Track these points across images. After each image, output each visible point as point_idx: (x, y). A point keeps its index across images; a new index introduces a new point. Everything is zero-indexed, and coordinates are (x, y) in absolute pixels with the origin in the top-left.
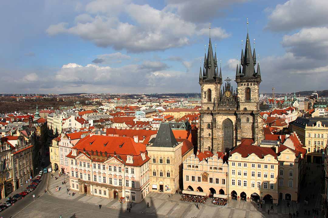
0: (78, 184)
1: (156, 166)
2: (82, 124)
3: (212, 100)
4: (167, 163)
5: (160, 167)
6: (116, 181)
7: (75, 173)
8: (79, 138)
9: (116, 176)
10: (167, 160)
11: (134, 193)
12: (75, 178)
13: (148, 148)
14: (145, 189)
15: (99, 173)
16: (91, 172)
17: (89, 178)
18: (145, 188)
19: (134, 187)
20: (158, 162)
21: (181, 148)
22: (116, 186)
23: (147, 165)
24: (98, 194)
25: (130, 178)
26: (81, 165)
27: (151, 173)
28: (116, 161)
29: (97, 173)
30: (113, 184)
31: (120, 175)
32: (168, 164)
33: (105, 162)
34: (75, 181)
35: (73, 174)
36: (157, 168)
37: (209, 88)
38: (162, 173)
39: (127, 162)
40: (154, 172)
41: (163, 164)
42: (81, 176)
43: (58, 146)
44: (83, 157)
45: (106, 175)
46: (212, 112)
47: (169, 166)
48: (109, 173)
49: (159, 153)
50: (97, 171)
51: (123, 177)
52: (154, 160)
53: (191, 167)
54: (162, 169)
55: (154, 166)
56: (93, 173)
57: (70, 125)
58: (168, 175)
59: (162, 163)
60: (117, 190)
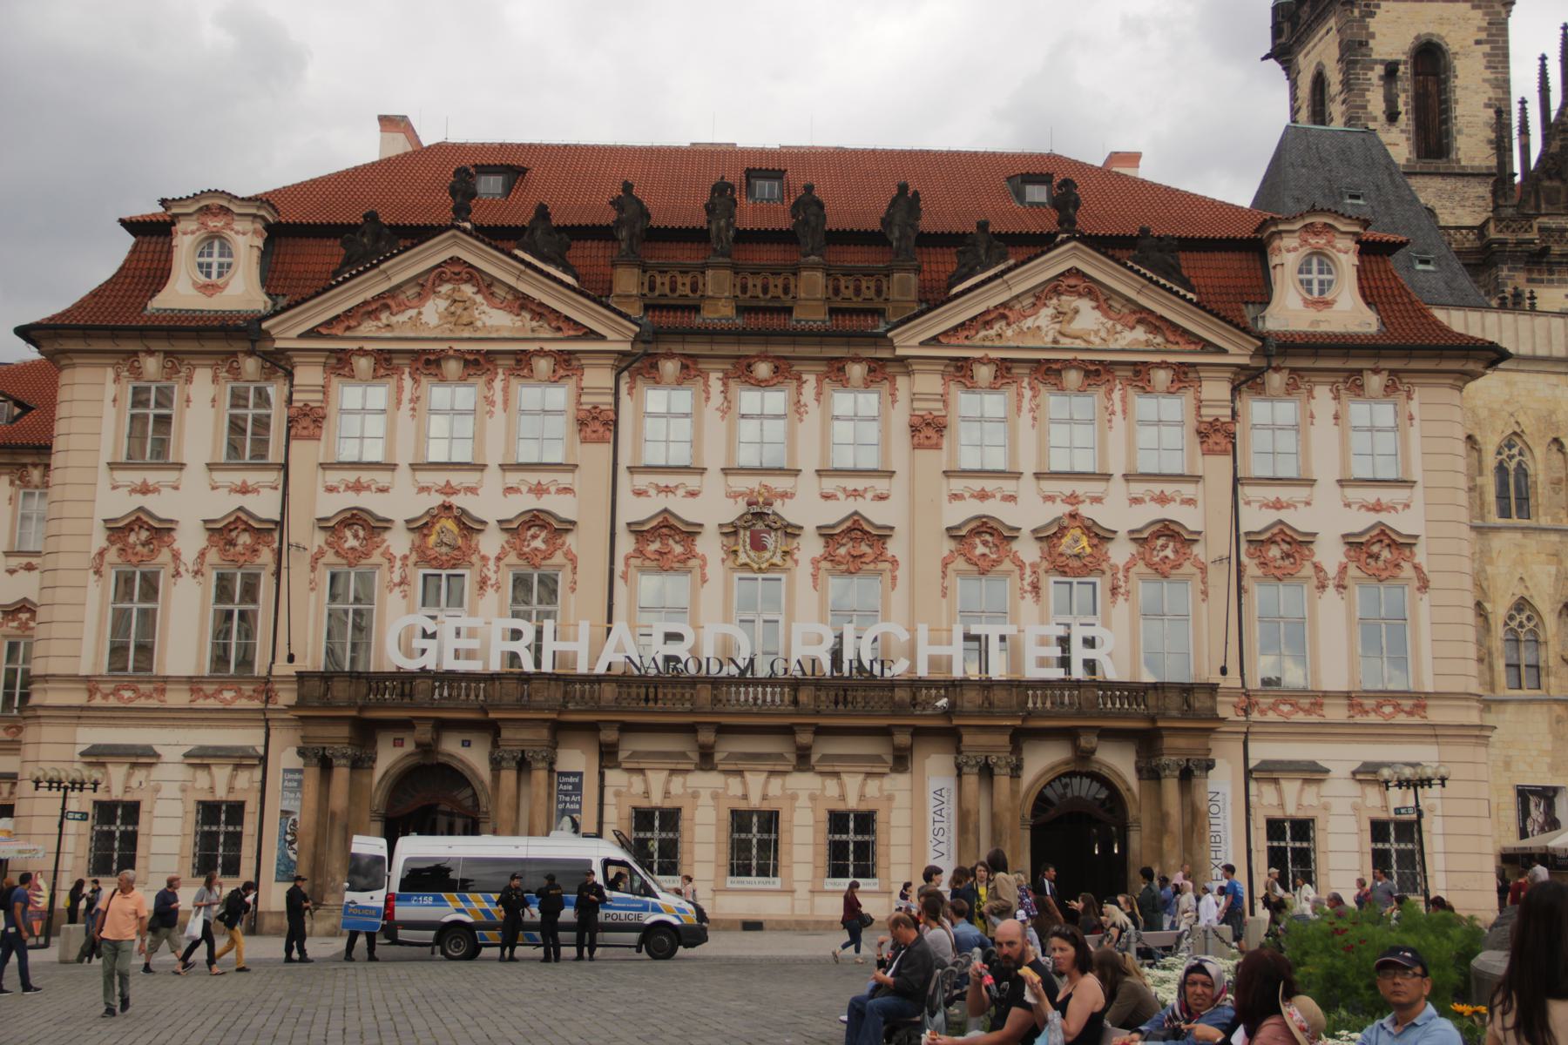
3: (1472, 147)
4: (1504, 512)
10: (1501, 469)
12: (177, 698)
15: (758, 527)
25: (1329, 554)
28: (1088, 318)
29: (710, 546)
31: (1172, 512)
32: (1515, 521)
33: (908, 342)
37: (1424, 30)
39: (1288, 311)
45: (894, 548)
46: (1493, 233)
47: (1532, 543)
48: (969, 509)
50: (712, 507)
51: (1217, 543)
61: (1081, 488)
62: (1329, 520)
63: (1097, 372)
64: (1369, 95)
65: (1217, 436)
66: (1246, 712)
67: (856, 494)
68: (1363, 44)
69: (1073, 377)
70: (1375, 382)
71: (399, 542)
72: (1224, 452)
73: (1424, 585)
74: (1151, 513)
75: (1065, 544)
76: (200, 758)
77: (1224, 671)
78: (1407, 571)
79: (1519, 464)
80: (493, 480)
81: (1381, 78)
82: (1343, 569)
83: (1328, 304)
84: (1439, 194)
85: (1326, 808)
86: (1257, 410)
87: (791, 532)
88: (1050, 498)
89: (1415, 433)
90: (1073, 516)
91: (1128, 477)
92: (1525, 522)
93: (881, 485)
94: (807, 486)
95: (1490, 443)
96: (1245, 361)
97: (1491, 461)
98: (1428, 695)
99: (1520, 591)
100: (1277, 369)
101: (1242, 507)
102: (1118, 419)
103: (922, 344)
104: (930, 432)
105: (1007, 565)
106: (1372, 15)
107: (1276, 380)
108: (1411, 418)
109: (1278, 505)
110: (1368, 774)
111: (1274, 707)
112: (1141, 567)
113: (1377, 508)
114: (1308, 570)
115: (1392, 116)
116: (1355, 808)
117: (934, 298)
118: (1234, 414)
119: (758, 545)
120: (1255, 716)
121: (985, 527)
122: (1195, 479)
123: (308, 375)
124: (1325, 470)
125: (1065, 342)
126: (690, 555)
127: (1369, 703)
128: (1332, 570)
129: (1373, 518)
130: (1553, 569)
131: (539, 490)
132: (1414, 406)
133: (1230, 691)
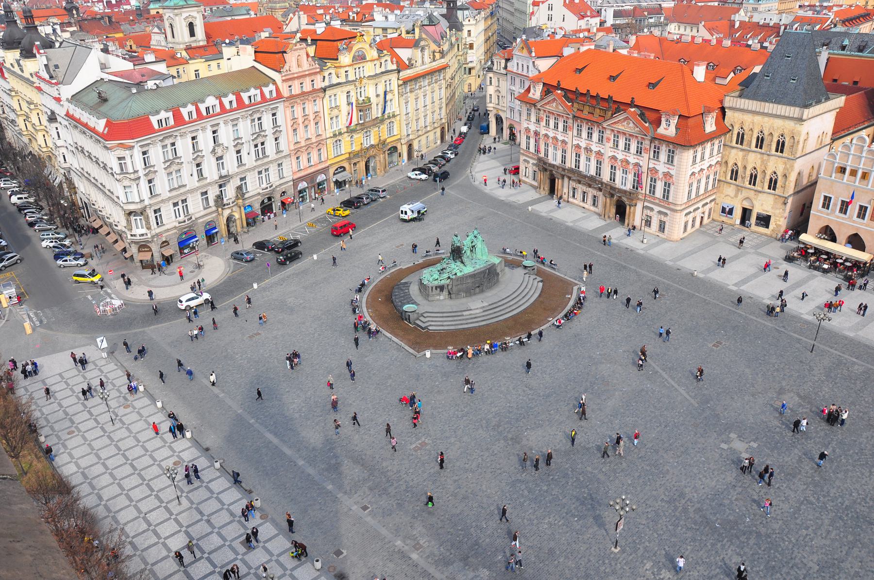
0: (537, 169)
1: (741, 154)
2: (583, 17)
4: (777, 151)
5: (754, 160)
7: (532, 141)
8: (560, 56)
10: (778, 142)
11: (666, 214)
13: (728, 102)
14: (700, 210)
15: (588, 150)
16: (569, 145)
17: (564, 158)
18: (698, 208)
19: (667, 198)
21: (834, 113)
22: (624, 188)
23: (716, 147)
24: (578, 201)
26: (548, 124)
27: (725, 172)
28: (631, 125)
29: (582, 150)
30: (618, 184)
32: (779, 154)
33: (605, 125)
34: (532, 161)
35: (528, 144)
38: (756, 176)
39: (661, 130)
40: (732, 171)
41: (763, 151)
42: (546, 151)
43: (504, 72)
44: (554, 104)
47: (780, 159)
49: (758, 119)
51: (645, 169)
52: (741, 139)
55: (737, 154)
57: (550, 18)
58: (773, 184)
59: (761, 148)
60: (624, 199)
74: (636, 161)
80: (560, 134)
87: (591, 151)
99: (774, 170)
110: (660, 212)
117: (612, 117)
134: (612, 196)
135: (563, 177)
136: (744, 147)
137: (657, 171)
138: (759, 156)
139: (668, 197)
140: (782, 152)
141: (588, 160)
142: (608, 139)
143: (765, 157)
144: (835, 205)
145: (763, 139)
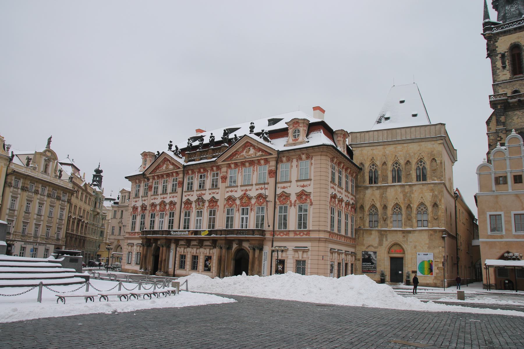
1: (377, 193)
5: (394, 194)
6: (245, 216)
9: (246, 198)
11: (305, 250)
12: (137, 236)
17: (171, 222)
20: (385, 179)
25: (293, 198)
27: (362, 219)
28: (252, 151)
29: (193, 205)
31: (263, 192)
32: (421, 182)
36: (382, 197)
44: (165, 166)
45: (219, 203)
47: (425, 188)
49: (390, 149)
50: (193, 198)
51: (271, 198)
53: (505, 182)
54: (401, 200)
55: (373, 194)
56: (183, 206)
60: (246, 245)
61: (248, 188)
62: (293, 190)
63: (252, 163)
64: (497, 63)
65: (273, 173)
66: (274, 236)
67: (214, 193)
68: (495, 50)
69: (247, 164)
70: (304, 157)
71: (158, 208)
72: (273, 177)
73: (311, 204)
74: (260, 192)
75: (244, 201)
76: (137, 245)
77: (269, 226)
78: (308, 201)
79: (424, 166)
81: (500, 58)
82: (296, 201)
83: (297, 140)
84: (520, 85)
85: (287, 257)
86: (282, 168)
87: (203, 201)
88: (242, 191)
89: (313, 167)
90: (245, 194)
91: (256, 184)
92: (424, 182)
93: (217, 191)
94: (207, 192)
95: (414, 162)
96: (276, 156)
97: (414, 166)
98: (310, 231)
100: (284, 157)
101: (277, 189)
102: (255, 172)
103: (223, 161)
104: (223, 179)
105: (234, 205)
106: (497, 42)
107: (284, 159)
108: (312, 164)
109: (284, 188)
110: (296, 250)
111: (279, 234)
112: (257, 204)
113: (303, 186)
114: (289, 202)
115: (504, 67)
116: (293, 257)
118: (277, 168)
119: (199, 205)
120: (276, 236)
121: (230, 198)
122: (268, 183)
123: (151, 180)
124: (294, 178)
125: (248, 157)
126: (191, 207)
127: (298, 233)
128: (293, 202)
129: (303, 188)
130: (431, 194)
131: (173, 197)
132: (313, 161)
133: (269, 231)
134: (229, 248)
135: (169, 248)
136: (379, 185)
137: (285, 196)
138: (399, 190)
139: (305, 224)
140: (425, 179)
141: (200, 214)
142: (224, 179)
143: (407, 189)
144: (508, 222)
145: (399, 171)
